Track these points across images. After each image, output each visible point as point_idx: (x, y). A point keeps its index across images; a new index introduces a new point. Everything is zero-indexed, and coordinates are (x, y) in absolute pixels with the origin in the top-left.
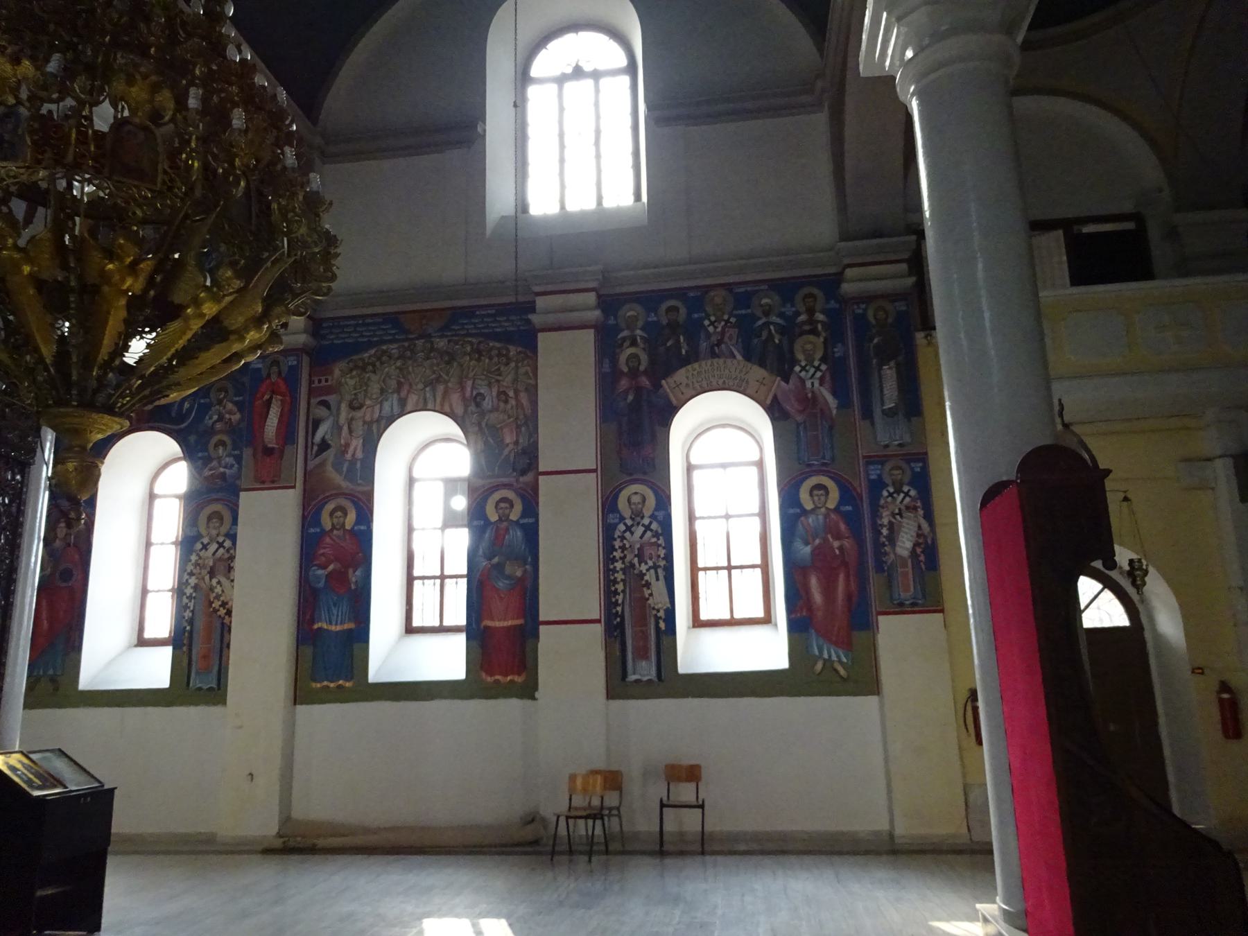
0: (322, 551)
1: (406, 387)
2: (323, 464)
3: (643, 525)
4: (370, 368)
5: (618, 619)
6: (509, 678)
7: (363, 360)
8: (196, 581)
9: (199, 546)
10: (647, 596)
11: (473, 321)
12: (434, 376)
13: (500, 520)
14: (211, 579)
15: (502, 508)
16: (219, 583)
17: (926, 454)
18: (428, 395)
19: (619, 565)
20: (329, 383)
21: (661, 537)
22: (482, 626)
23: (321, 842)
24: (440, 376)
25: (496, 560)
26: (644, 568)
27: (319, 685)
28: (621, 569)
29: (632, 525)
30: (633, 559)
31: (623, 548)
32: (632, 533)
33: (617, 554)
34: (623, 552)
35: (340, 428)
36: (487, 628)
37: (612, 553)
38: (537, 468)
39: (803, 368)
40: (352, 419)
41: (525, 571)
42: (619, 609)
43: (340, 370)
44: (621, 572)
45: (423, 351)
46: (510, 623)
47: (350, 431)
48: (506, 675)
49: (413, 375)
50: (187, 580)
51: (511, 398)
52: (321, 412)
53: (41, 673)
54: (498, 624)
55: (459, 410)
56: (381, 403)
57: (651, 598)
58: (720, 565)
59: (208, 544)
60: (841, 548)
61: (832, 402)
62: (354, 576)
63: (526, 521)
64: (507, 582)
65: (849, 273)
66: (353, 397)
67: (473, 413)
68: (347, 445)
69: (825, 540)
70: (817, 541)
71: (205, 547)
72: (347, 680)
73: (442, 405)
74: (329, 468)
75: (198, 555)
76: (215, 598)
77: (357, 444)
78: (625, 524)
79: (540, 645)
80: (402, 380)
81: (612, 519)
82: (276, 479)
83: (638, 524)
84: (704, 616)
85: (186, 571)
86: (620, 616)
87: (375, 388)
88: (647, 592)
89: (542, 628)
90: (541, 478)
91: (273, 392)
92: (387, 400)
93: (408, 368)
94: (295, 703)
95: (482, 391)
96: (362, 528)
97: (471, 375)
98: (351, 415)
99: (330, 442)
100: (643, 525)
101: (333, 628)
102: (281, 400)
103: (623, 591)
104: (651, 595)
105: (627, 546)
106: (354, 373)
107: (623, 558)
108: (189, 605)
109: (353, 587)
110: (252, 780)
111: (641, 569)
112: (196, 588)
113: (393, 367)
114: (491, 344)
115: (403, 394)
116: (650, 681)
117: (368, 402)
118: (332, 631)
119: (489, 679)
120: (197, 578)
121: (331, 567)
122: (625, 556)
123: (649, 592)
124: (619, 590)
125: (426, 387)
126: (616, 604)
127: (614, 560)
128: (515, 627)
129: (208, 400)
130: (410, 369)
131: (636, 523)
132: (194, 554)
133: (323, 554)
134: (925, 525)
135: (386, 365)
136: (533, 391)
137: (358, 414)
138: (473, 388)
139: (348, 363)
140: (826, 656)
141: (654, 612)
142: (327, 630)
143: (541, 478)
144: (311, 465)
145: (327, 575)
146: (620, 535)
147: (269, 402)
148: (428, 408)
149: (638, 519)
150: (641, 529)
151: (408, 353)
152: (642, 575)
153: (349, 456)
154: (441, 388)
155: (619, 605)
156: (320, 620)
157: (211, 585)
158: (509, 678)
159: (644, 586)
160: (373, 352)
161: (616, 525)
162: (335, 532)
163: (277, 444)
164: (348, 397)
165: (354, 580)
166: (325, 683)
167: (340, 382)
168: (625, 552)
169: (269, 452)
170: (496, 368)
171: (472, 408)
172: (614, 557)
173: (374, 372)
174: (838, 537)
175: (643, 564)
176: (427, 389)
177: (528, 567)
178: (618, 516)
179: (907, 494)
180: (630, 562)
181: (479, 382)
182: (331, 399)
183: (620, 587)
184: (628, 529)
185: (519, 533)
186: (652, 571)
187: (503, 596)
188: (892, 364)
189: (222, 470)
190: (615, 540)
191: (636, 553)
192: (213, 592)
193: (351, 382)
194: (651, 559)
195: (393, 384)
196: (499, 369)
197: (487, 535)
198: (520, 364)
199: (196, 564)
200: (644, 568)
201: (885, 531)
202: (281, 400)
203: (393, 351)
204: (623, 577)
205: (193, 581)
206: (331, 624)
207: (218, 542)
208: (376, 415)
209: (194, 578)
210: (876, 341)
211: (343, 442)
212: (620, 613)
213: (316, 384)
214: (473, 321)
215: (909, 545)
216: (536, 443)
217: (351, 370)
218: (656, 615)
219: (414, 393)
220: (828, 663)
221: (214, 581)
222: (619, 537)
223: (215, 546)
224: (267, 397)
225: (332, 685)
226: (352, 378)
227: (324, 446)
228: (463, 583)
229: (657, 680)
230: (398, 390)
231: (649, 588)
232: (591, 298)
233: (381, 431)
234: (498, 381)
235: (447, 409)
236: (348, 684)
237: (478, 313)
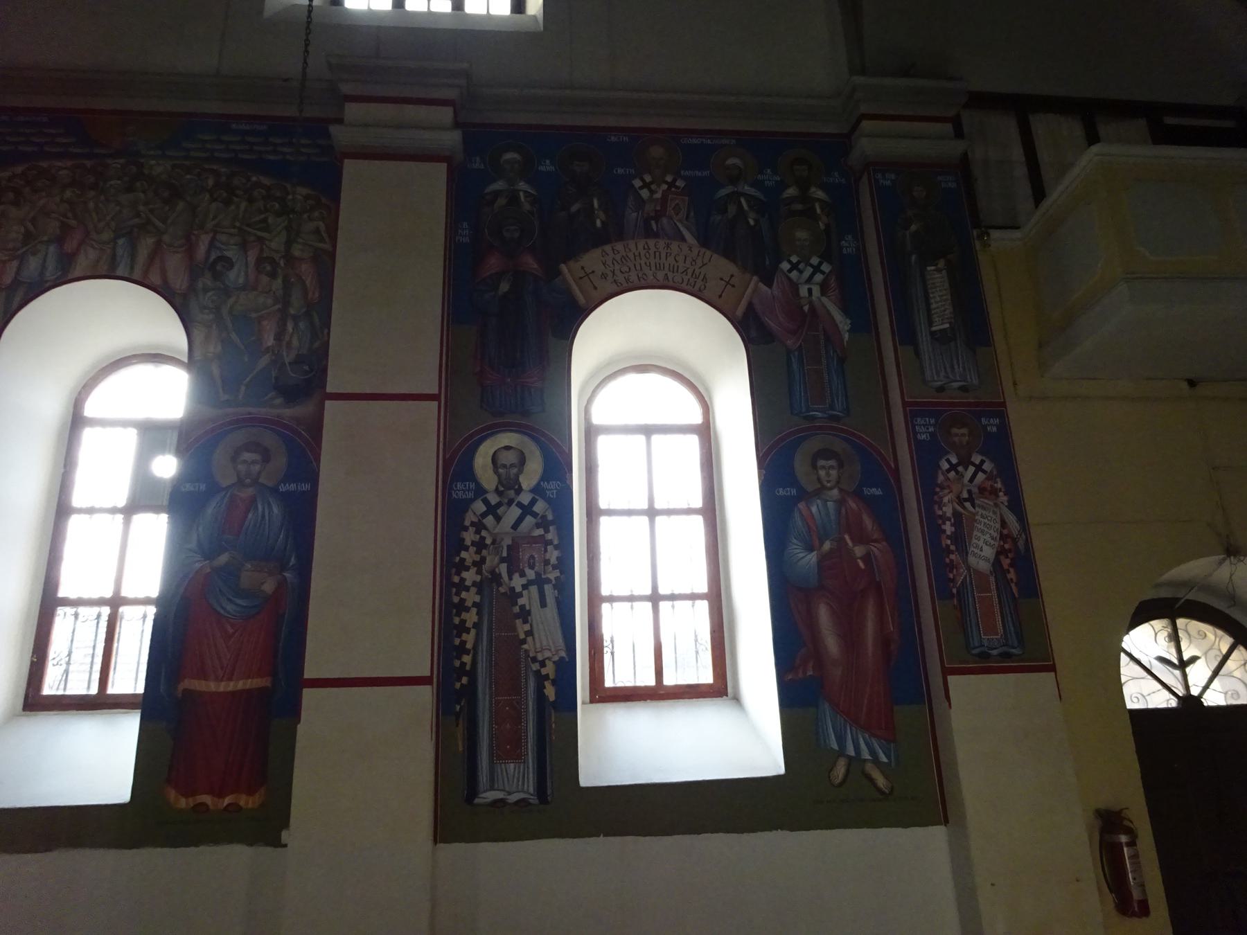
3: (520, 505)
4: (11, 195)
5: (465, 680)
6: (227, 801)
10: (522, 636)
11: (225, 138)
12: (137, 220)
13: (240, 483)
15: (245, 462)
17: (1003, 404)
18: (120, 252)
19: (470, 576)
21: (551, 528)
25: (223, 559)
26: (517, 582)
28: (474, 584)
29: (499, 505)
30: (498, 565)
31: (480, 545)
32: (498, 519)
33: (468, 556)
34: (478, 552)
36: (185, 690)
37: (458, 554)
38: (324, 386)
39: (794, 267)
42: (467, 659)
44: (473, 590)
48: (221, 795)
49: (94, 215)
54: (212, 686)
55: (179, 282)
56: (22, 259)
57: (529, 639)
58: (638, 592)
60: (867, 558)
61: (843, 323)
63: (292, 487)
65: (866, 125)
67: (206, 290)
69: (841, 541)
70: (827, 546)
73: (146, 273)
78: (486, 502)
79: (301, 729)
80: (73, 223)
81: (461, 491)
83: (510, 503)
86: (467, 674)
88: (522, 629)
89: (308, 694)
90: (328, 403)
92: (34, 254)
95: (229, 254)
97: (210, 225)
100: (520, 505)
103: (476, 625)
104: (530, 633)
105: (488, 541)
107: (479, 564)
111: (513, 584)
114: (254, 179)
115: (70, 246)
116: (522, 803)
119: (183, 803)
122: (483, 560)
123: (527, 627)
124: (469, 624)
126: (462, 649)
127: (462, 566)
128: (248, 692)
130: (91, 205)
131: (506, 501)
134: (1011, 519)
135: (44, 194)
136: (325, 264)
138: (212, 245)
140: (851, 751)
141: (535, 667)
143: (328, 403)
146: (475, 520)
149: (511, 493)
150: (515, 512)
152: (513, 596)
154: (146, 245)
155: (467, 652)
158: (227, 801)
159: (517, 616)
160: (19, 169)
161: (472, 501)
168: (484, 552)
171: (206, 280)
172: (463, 560)
174: (861, 539)
175: (516, 576)
176: (121, 242)
178: (473, 486)
179: (979, 468)
180: (493, 572)
181: (223, 238)
183: (471, 617)
184: (492, 510)
185: (275, 510)
186: (534, 589)
187: (231, 631)
188: (941, 264)
190: (466, 529)
191: (505, 554)
194: (532, 567)
196: (265, 220)
197: (210, 511)
198: (305, 216)
200: (517, 582)
201: (948, 528)
204: (477, 599)
210: (913, 228)
212: (468, 668)
214: (225, 138)
215: (989, 552)
216: (326, 345)
218: (538, 673)
219: (93, 247)
220: (855, 762)
222: (473, 524)
229: (537, 802)
230: (60, 240)
231: (525, 622)
232: (446, 115)
233: (15, 305)
234: (261, 240)
235: (155, 279)
237: (234, 126)
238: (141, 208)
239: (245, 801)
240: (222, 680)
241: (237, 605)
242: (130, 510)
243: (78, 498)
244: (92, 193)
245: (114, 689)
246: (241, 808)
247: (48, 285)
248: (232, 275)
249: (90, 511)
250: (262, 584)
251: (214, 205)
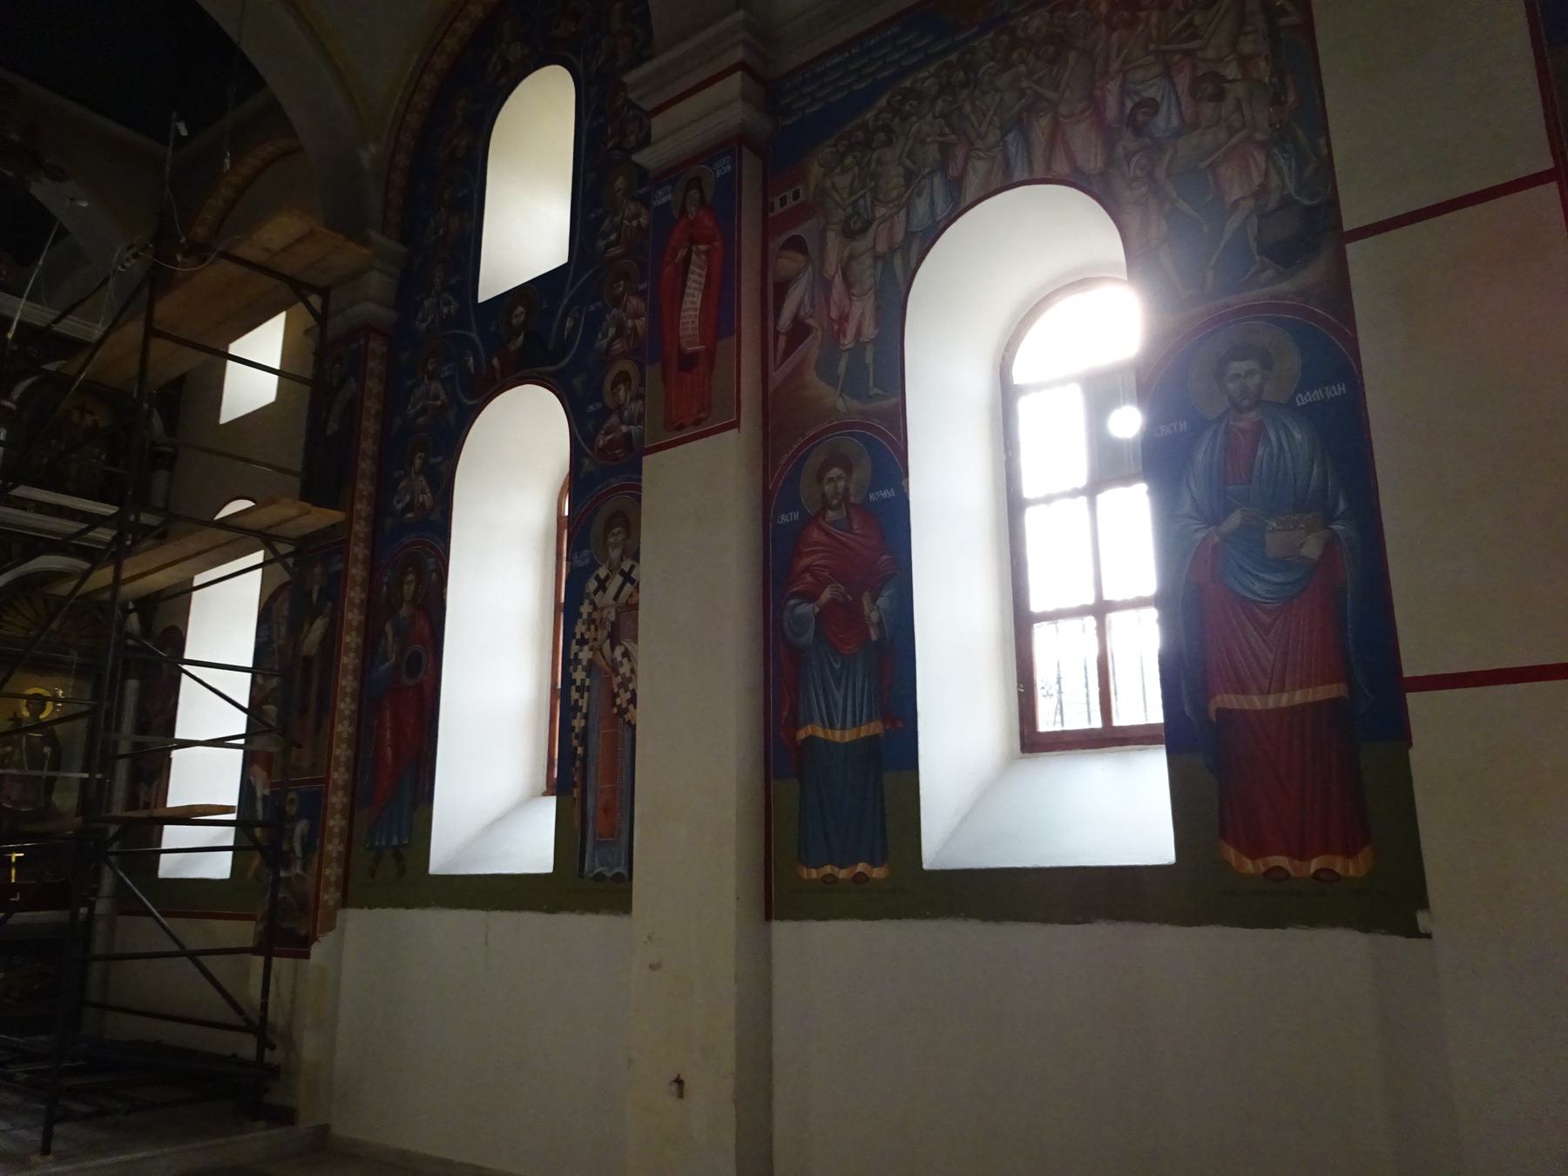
0: (805, 561)
1: (960, 153)
4: (881, 136)
6: (1315, 865)
8: (590, 655)
9: (592, 585)
14: (613, 649)
15: (1237, 376)
16: (626, 654)
18: (1012, 150)
22: (1212, 708)
25: (1235, 519)
27: (814, 874)
35: (827, 285)
36: (1219, 711)
38: (1339, 224)
40: (852, 257)
41: (1330, 546)
43: (822, 166)
45: (992, 59)
46: (1299, 697)
47: (848, 285)
48: (1303, 855)
50: (576, 654)
51: (1234, 81)
52: (788, 263)
53: (383, 843)
55: (1092, 160)
56: (909, 207)
59: (607, 577)
62: (875, 610)
63: (1317, 395)
64: (1278, 579)
66: (850, 210)
67: (1128, 157)
68: (844, 318)
71: (602, 586)
72: (873, 864)
73: (1049, 168)
74: (811, 377)
75: (592, 603)
76: (620, 685)
77: (862, 311)
79: (1414, 754)
82: (703, 415)
85: (574, 636)
89: (1415, 702)
90: (1352, 249)
91: (693, 240)
92: (919, 195)
94: (768, 916)
95: (1150, 93)
96: (886, 494)
98: (846, 253)
99: (810, 321)
101: (837, 736)
102: (707, 253)
106: (849, 160)
108: (580, 703)
110: (681, 1095)
112: (591, 668)
113: (929, 117)
118: (836, 744)
119: (1249, 866)
120: (591, 649)
121: (826, 595)
125: (1004, 135)
128: (1316, 706)
129: (599, 304)
130: (967, 108)
132: (587, 602)
133: (808, 569)
135: (914, 118)
137: (862, 244)
138: (1124, 92)
142: (826, 742)
143: (1352, 249)
144: (777, 377)
145: (818, 616)
147: (687, 261)
148: (1016, 179)
153: (848, 341)
154: (1042, 125)
156: (811, 721)
157: (613, 660)
158: (1315, 865)
160: (883, 102)
162: (831, 514)
165: (874, 617)
166: (828, 869)
169: (688, 362)
170: (1184, 21)
171: (1128, 141)
176: (1010, 137)
177: (1337, 527)
181: (1139, 75)
182: (805, 230)
185: (1298, 436)
187: (1267, 620)
189: (624, 428)
192: (617, 673)
193: (843, 181)
195: (932, 153)
196: (1190, 24)
197: (1200, 456)
199: (591, 621)
202: (707, 253)
205: (585, 655)
206: (832, 727)
207: (622, 573)
208: (899, 236)
209: (586, 648)
211: (834, 314)
213: (778, 209)
219: (980, 158)
221: (619, 651)
223: (618, 579)
224: (682, 253)
225: (843, 874)
226: (844, 172)
227: (800, 331)
228: (1150, 618)
230: (942, 167)
233: (913, 262)
234: (1188, 53)
235: (1062, 167)
236: (878, 873)
238: (1024, 84)
239: (1338, 864)
240: (1269, 693)
241: (1268, 582)
242: (1094, 488)
243: (1029, 490)
244: (965, 92)
245: (1124, 717)
246: (1338, 877)
248: (1160, 121)
249: (1048, 500)
250: (1302, 546)
251: (1115, 36)
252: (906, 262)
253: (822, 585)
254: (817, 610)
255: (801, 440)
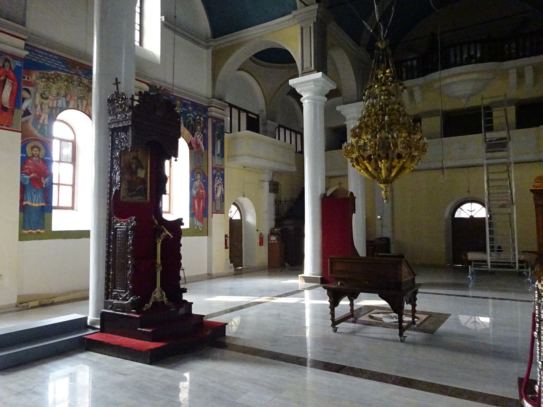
0: (27, 166)
1: (69, 97)
2: (27, 121)
4: (52, 80)
7: (48, 74)
17: (224, 169)
20: (30, 80)
23: (56, 300)
24: (85, 96)
27: (27, 232)
35: (36, 107)
39: (197, 134)
47: (41, 109)
52: (25, 94)
56: (57, 100)
60: (202, 193)
61: (203, 148)
62: (45, 181)
66: (43, 92)
68: (40, 116)
69: (199, 189)
70: (197, 190)
72: (41, 229)
74: (30, 124)
80: (67, 92)
84: (70, 205)
87: (54, 92)
91: (7, 76)
93: (70, 87)
99: (31, 112)
101: (34, 205)
106: (43, 80)
109: (44, 186)
115: (68, 99)
117: (50, 97)
118: (33, 206)
121: (32, 175)
125: (78, 99)
130: (71, 88)
133: (27, 168)
134: (223, 189)
137: (46, 102)
139: (40, 73)
140: (197, 225)
145: (30, 179)
151: (70, 80)
153: (41, 121)
156: (26, 200)
160: (53, 72)
163: (10, 106)
164: (40, 91)
165: (44, 182)
166: (30, 231)
167: (36, 83)
173: (54, 83)
174: (202, 189)
176: (79, 100)
179: (220, 180)
188: (220, 140)
193: (43, 84)
195: (63, 92)
201: (215, 189)
203: (63, 76)
206: (32, 202)
208: (55, 105)
210: (217, 132)
215: (220, 194)
217: (42, 78)
220: (198, 226)
225: (34, 232)
226: (42, 82)
230: (65, 96)
233: (57, 113)
236: (42, 231)
244: (71, 85)
247: (64, 109)
252: (56, 112)
253: (31, 173)
254: (30, 178)
255: (26, 139)
